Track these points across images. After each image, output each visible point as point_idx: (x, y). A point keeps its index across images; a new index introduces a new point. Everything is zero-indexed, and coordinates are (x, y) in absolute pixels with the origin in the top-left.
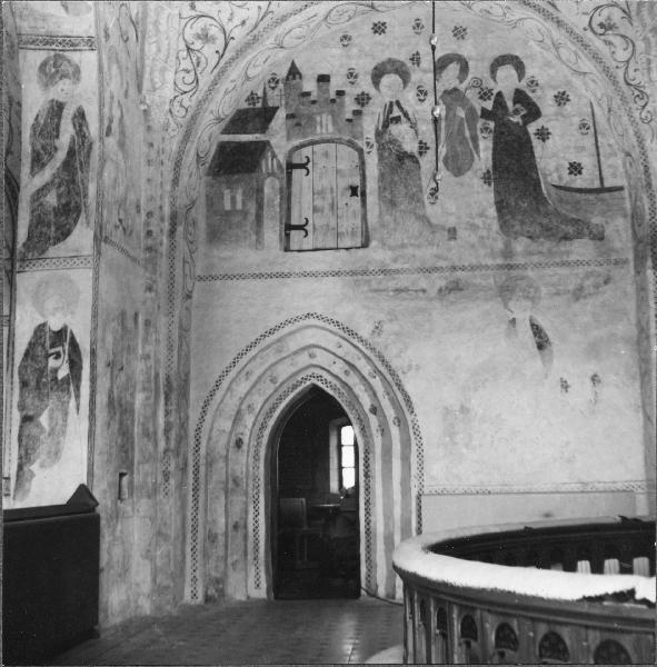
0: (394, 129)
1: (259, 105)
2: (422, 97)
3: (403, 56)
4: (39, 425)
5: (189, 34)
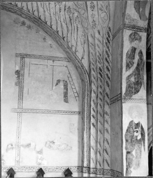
4: (132, 155)
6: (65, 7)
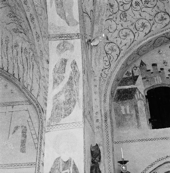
1: (131, 76)
5: (107, 48)
6: (22, 49)
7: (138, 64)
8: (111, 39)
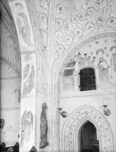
0: (101, 63)
1: (72, 61)
2: (108, 56)
3: (103, 48)
4: (25, 132)
5: (57, 48)
7: (77, 54)
8: (59, 43)
